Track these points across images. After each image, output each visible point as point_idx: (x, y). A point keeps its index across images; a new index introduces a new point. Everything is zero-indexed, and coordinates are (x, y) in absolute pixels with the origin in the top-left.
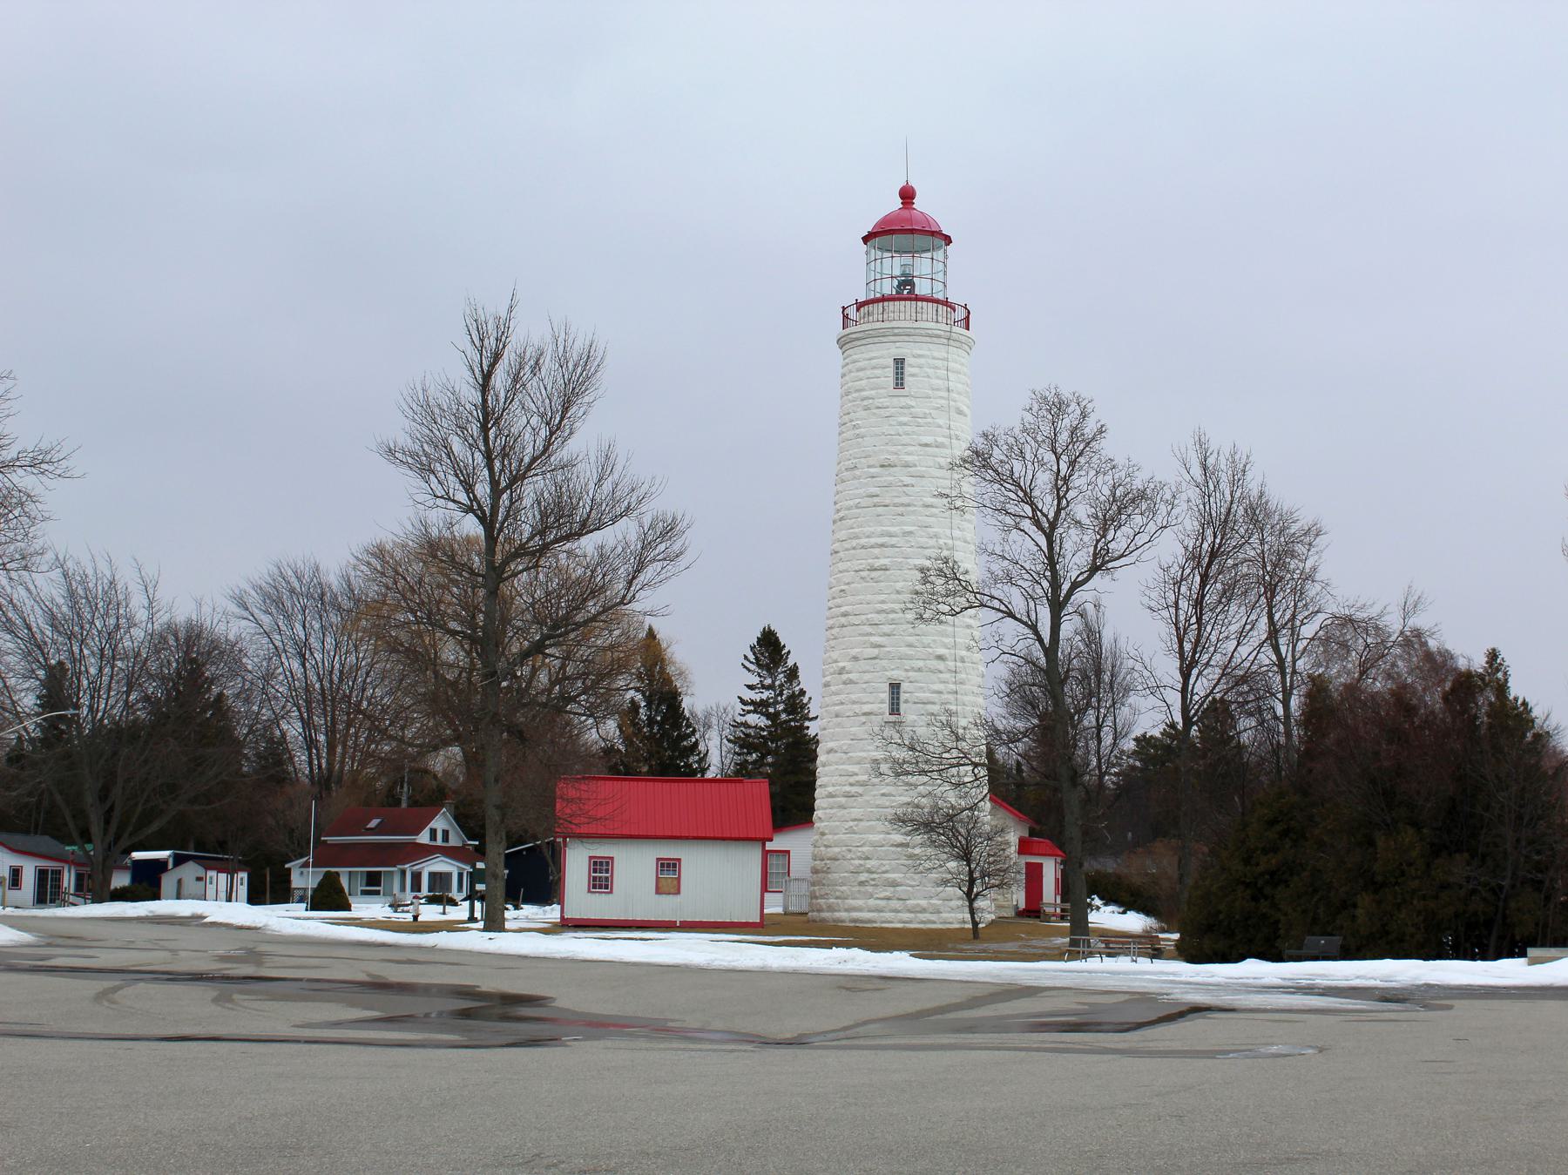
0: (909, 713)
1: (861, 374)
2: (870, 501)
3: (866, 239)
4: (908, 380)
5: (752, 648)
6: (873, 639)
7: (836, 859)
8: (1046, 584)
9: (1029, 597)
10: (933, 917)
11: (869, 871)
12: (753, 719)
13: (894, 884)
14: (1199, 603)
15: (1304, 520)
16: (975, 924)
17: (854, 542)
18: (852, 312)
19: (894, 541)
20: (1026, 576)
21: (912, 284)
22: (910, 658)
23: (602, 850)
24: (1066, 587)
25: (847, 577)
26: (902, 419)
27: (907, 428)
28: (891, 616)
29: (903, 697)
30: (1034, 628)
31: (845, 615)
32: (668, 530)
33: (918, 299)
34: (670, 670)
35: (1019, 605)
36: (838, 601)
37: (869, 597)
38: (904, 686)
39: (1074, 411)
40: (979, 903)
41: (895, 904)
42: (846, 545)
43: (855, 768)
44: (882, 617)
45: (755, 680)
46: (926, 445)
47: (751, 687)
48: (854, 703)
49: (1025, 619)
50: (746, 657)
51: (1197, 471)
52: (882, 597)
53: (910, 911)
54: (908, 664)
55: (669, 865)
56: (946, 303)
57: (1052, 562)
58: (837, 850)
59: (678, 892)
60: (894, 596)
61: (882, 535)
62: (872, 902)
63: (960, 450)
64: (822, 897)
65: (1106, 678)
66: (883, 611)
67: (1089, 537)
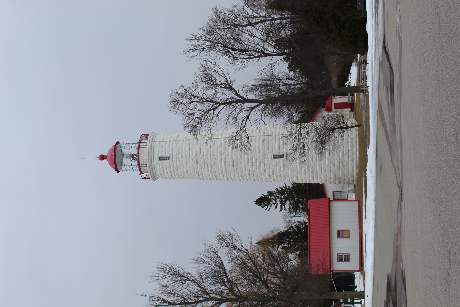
0: (283, 151)
1: (165, 172)
2: (210, 167)
3: (118, 172)
4: (167, 156)
5: (262, 207)
6: (258, 165)
7: (335, 175)
8: (237, 105)
9: (241, 110)
10: (355, 140)
12: (287, 206)
13: (343, 155)
14: (242, 51)
15: (211, 14)
16: (356, 126)
17: (224, 172)
18: (144, 176)
19: (223, 159)
20: (234, 112)
21: (133, 155)
22: (264, 152)
23: (335, 258)
24: (237, 98)
25: (236, 174)
26: (181, 156)
27: (184, 155)
28: (249, 159)
29: (277, 154)
30: (252, 109)
31: (249, 175)
32: (222, 238)
33: (138, 153)
34: (271, 236)
35: (244, 114)
36: (245, 177)
37: (243, 166)
38: (274, 153)
39: (176, 97)
40: (349, 125)
41: (350, 154)
42: (225, 175)
43: (303, 170)
44: (250, 162)
45: (273, 206)
46: (189, 148)
47: (276, 208)
48: (280, 171)
49: (249, 112)
50: (266, 209)
51: (196, 53)
52: (243, 162)
53: (353, 149)
54: (266, 152)
55: (340, 234)
56: (140, 143)
57: (229, 103)
58: (332, 175)
59: (349, 230)
60: (243, 158)
61: (221, 163)
62: (350, 162)
63: (190, 136)
64: (349, 180)
65: (269, 83)
66: (248, 161)
67: (220, 90)
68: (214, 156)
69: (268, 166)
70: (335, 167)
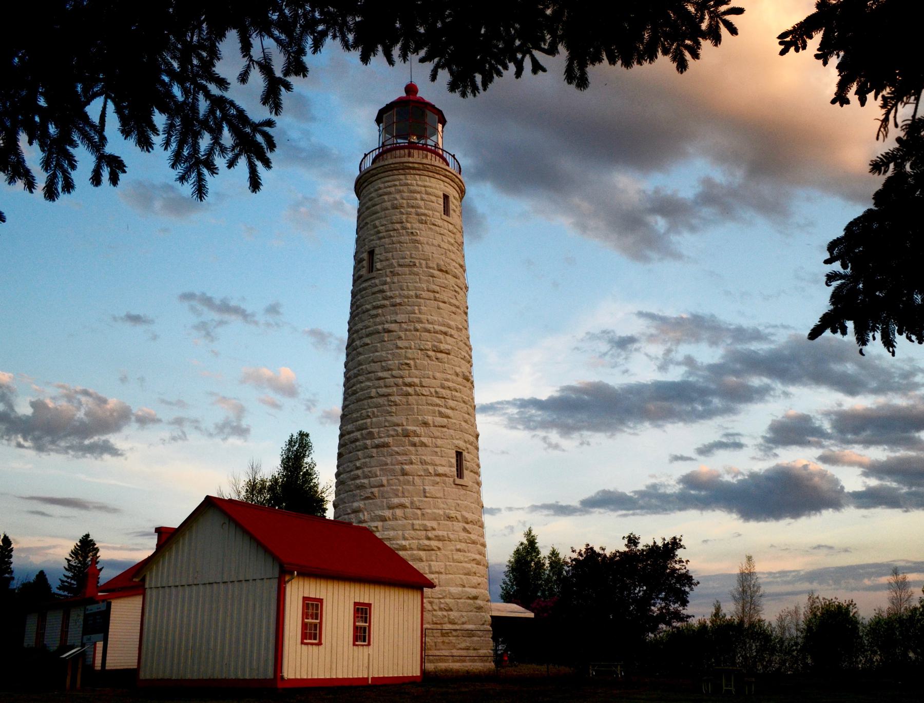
11: (452, 622)
26: (452, 241)
38: (465, 453)
43: (434, 524)
60: (455, 378)
61: (444, 325)
62: (455, 652)
68: (454, 313)
69: (438, 434)
70: (441, 609)
